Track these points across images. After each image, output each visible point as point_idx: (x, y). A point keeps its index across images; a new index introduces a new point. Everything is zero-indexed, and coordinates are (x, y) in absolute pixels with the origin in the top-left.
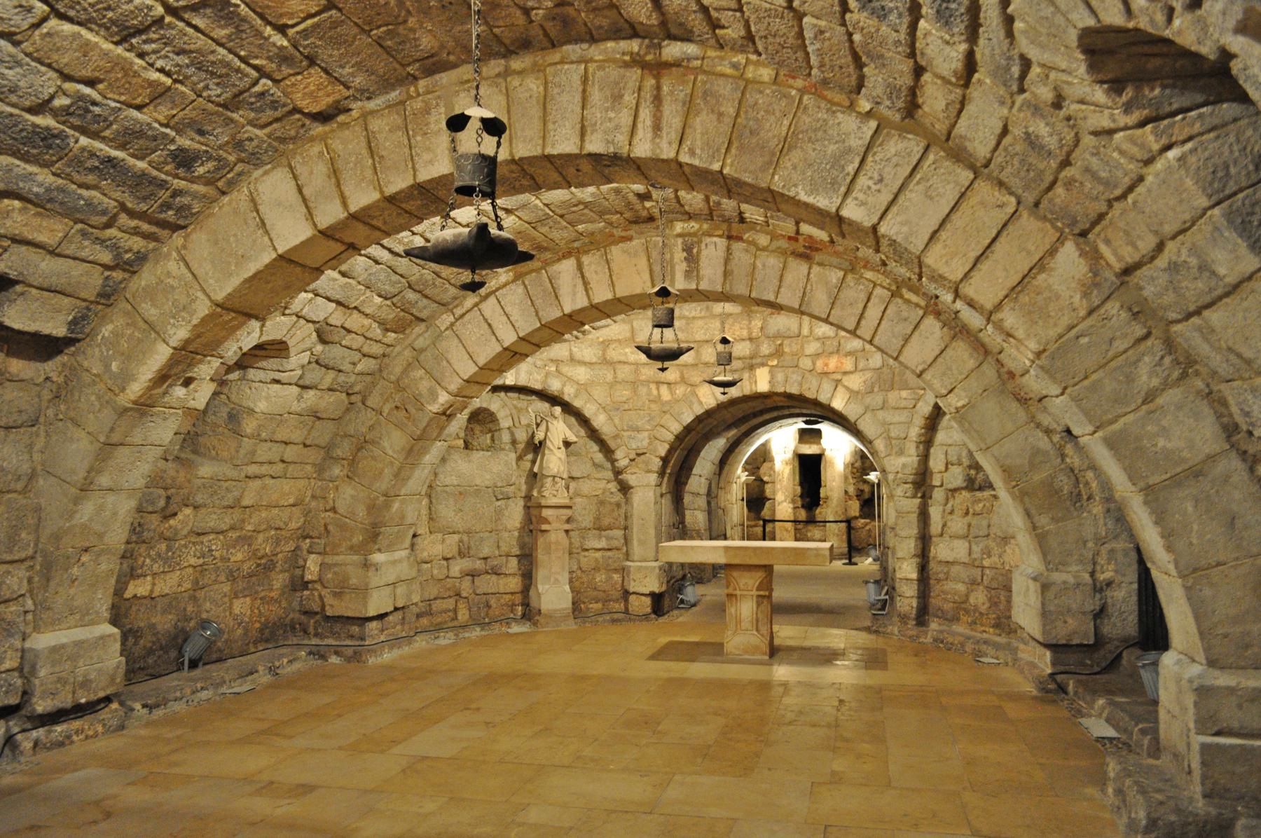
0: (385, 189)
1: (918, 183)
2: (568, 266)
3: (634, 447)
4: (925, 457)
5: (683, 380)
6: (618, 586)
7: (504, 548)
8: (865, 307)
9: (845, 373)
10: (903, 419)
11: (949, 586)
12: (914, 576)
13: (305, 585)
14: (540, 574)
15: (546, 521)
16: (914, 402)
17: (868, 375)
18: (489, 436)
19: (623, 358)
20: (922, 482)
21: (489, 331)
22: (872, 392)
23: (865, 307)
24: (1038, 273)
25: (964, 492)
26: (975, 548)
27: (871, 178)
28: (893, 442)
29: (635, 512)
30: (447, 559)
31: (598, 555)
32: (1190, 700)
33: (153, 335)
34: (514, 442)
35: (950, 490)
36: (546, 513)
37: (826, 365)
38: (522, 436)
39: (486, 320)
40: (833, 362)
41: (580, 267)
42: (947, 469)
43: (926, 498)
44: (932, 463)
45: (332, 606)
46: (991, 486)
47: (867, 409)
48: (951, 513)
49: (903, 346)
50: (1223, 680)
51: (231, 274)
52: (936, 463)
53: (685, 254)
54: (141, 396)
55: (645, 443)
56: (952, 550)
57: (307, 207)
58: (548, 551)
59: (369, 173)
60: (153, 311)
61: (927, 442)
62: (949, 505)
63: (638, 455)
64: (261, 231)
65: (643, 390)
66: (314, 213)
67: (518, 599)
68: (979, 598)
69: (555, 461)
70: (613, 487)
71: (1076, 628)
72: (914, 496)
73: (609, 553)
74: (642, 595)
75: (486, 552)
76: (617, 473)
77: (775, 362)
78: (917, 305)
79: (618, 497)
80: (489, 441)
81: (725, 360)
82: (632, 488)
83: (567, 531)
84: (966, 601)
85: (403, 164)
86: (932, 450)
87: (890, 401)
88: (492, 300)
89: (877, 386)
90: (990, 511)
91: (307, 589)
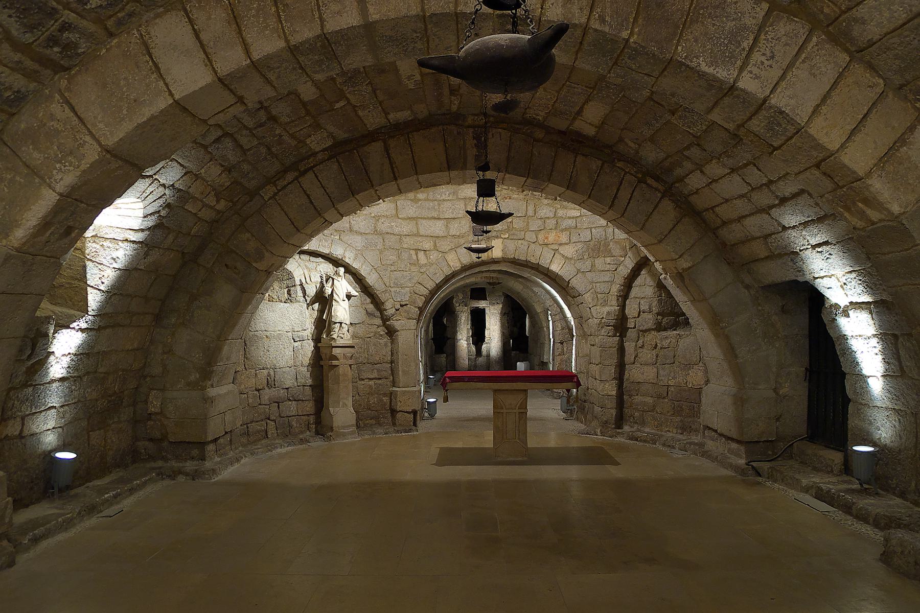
0: (290, 38)
1: (804, 61)
2: (376, 148)
3: (399, 300)
4: (623, 307)
7: (301, 381)
8: (618, 190)
9: (561, 244)
11: (638, 399)
12: (614, 393)
14: (331, 400)
15: (336, 358)
17: (580, 246)
18: (286, 290)
19: (389, 231)
20: (620, 326)
21: (308, 201)
23: (618, 190)
24: (901, 146)
25: (653, 332)
26: (661, 372)
27: (764, 54)
30: (258, 390)
31: (372, 383)
35: (641, 331)
36: (336, 351)
37: (547, 238)
38: (312, 291)
39: (305, 192)
40: (552, 237)
41: (387, 150)
42: (639, 315)
47: (578, 271)
49: (647, 220)
51: (123, 119)
52: (631, 309)
53: (475, 141)
54: (24, 244)
59: (272, 22)
60: (36, 155)
61: (624, 296)
62: (640, 342)
63: (402, 306)
64: (155, 75)
65: (405, 256)
66: (214, 59)
67: (312, 419)
69: (342, 311)
70: (382, 331)
72: (615, 336)
73: (380, 382)
74: (407, 412)
76: (385, 320)
77: (507, 236)
78: (657, 189)
79: (386, 339)
80: (286, 295)
82: (398, 331)
83: (350, 366)
85: (310, 14)
87: (597, 265)
88: (310, 175)
89: (587, 254)
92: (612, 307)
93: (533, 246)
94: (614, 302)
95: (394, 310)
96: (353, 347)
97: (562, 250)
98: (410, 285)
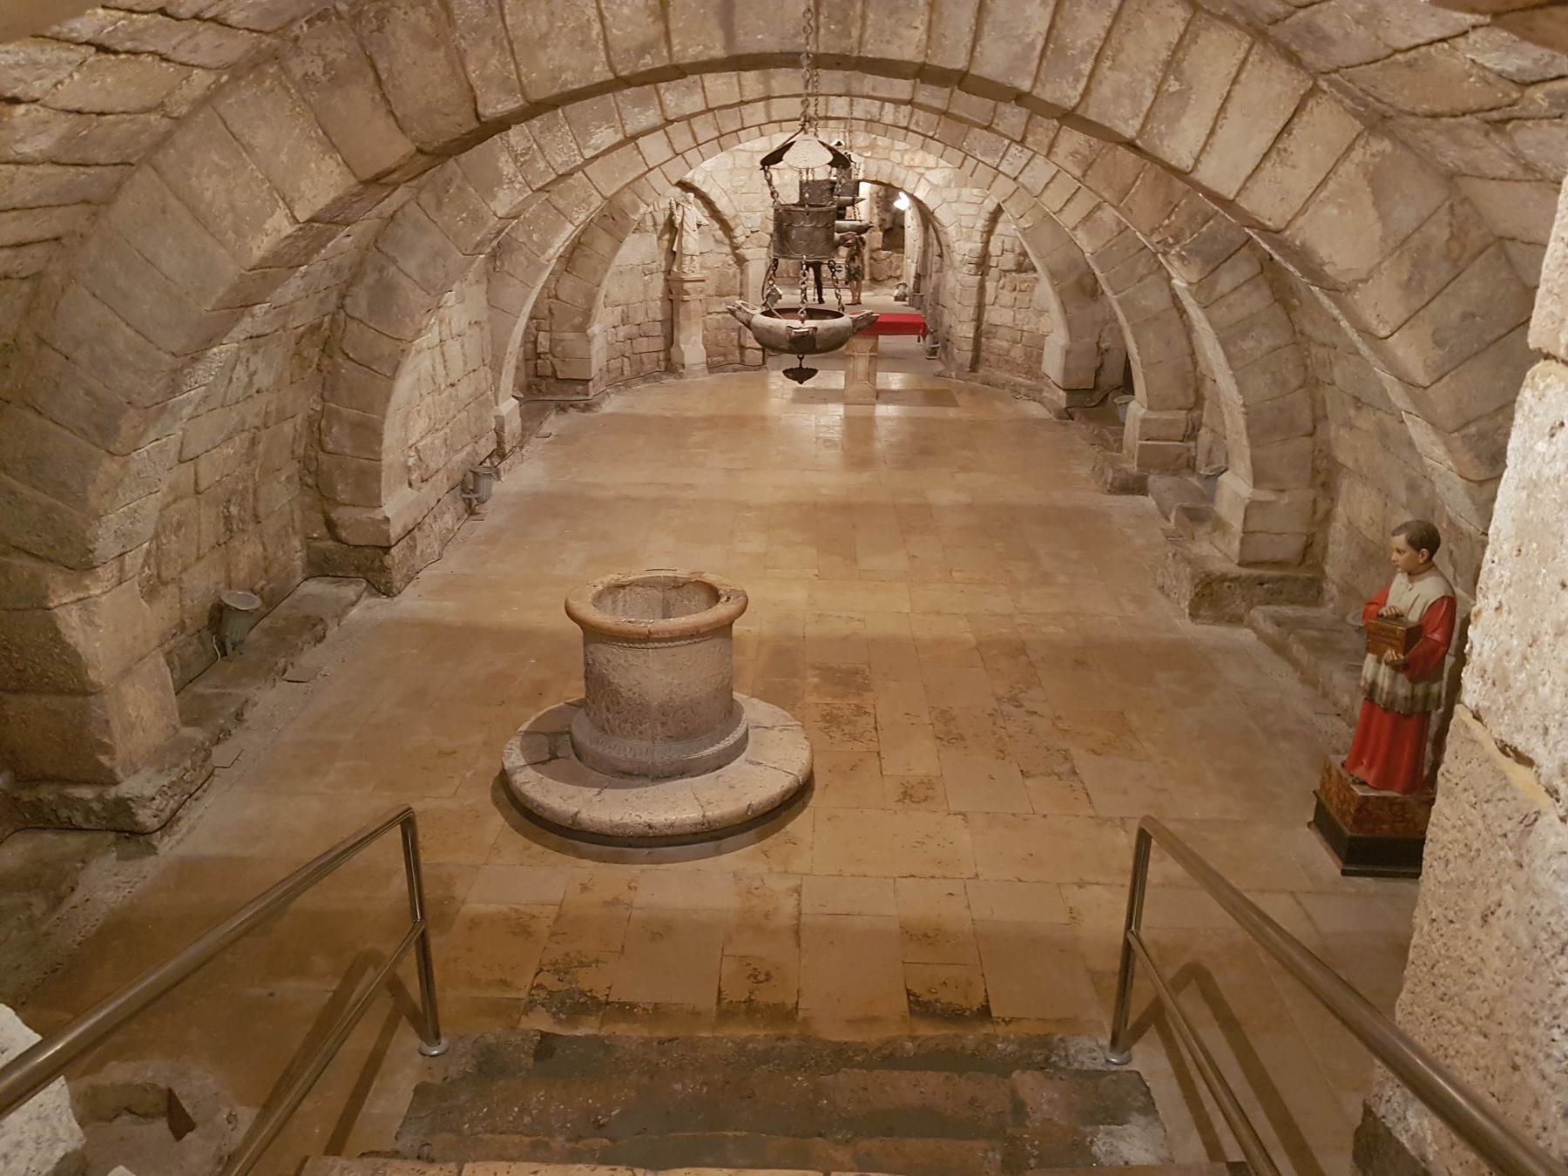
4: (987, 243)
6: (735, 343)
7: (651, 315)
9: (928, 168)
10: (972, 212)
11: (996, 342)
12: (971, 335)
13: (538, 356)
16: (982, 199)
20: (982, 263)
22: (948, 186)
26: (1018, 316)
28: (964, 230)
29: (750, 282)
31: (719, 316)
32: (1138, 424)
33: (562, 218)
34: (655, 224)
36: (687, 286)
37: (913, 160)
38: (661, 219)
42: (1002, 253)
44: (991, 248)
45: (562, 371)
46: (1035, 270)
47: (944, 200)
48: (1003, 288)
50: (1153, 416)
52: (994, 248)
55: (759, 224)
56: (1001, 316)
57: (669, 138)
58: (689, 318)
60: (561, 201)
61: (989, 232)
62: (1001, 282)
63: (752, 232)
67: (662, 356)
68: (1017, 353)
69: (691, 241)
70: (730, 260)
71: (1085, 378)
72: (976, 274)
75: (640, 318)
76: (735, 247)
77: (869, 154)
79: (735, 268)
84: (1008, 354)
86: (992, 238)
90: (1032, 290)
91: (539, 358)
92: (976, 245)
93: (897, 169)
94: (978, 238)
95: (744, 238)
96: (703, 281)
97: (928, 175)
98: (761, 209)
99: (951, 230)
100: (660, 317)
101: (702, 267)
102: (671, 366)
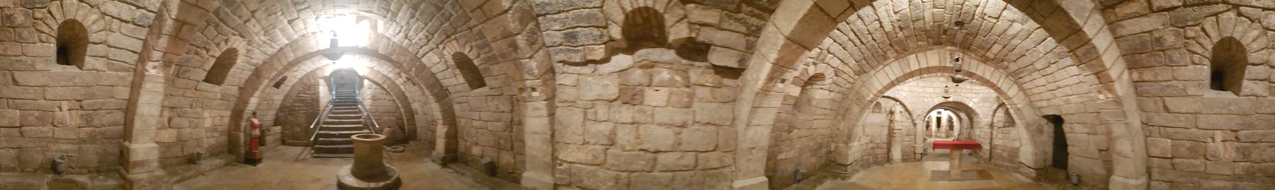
4: (993, 119)
5: (931, 97)
7: (883, 141)
11: (997, 151)
15: (895, 133)
34: (886, 111)
36: (895, 131)
38: (888, 110)
43: (992, 128)
61: (994, 116)
67: (886, 155)
69: (897, 117)
70: (912, 124)
76: (913, 120)
79: (913, 127)
81: (946, 92)
99: (981, 115)
100: (886, 142)
101: (902, 126)
102: (889, 160)
